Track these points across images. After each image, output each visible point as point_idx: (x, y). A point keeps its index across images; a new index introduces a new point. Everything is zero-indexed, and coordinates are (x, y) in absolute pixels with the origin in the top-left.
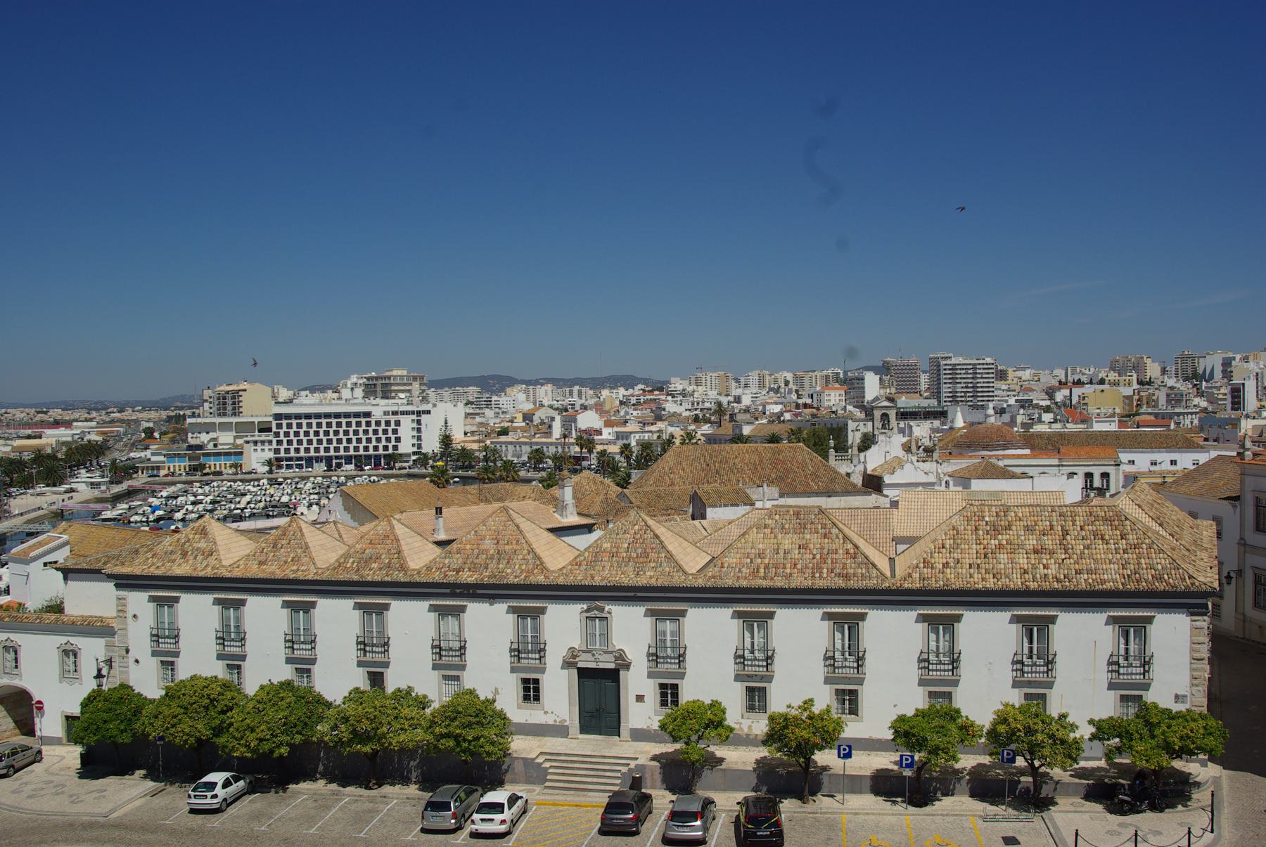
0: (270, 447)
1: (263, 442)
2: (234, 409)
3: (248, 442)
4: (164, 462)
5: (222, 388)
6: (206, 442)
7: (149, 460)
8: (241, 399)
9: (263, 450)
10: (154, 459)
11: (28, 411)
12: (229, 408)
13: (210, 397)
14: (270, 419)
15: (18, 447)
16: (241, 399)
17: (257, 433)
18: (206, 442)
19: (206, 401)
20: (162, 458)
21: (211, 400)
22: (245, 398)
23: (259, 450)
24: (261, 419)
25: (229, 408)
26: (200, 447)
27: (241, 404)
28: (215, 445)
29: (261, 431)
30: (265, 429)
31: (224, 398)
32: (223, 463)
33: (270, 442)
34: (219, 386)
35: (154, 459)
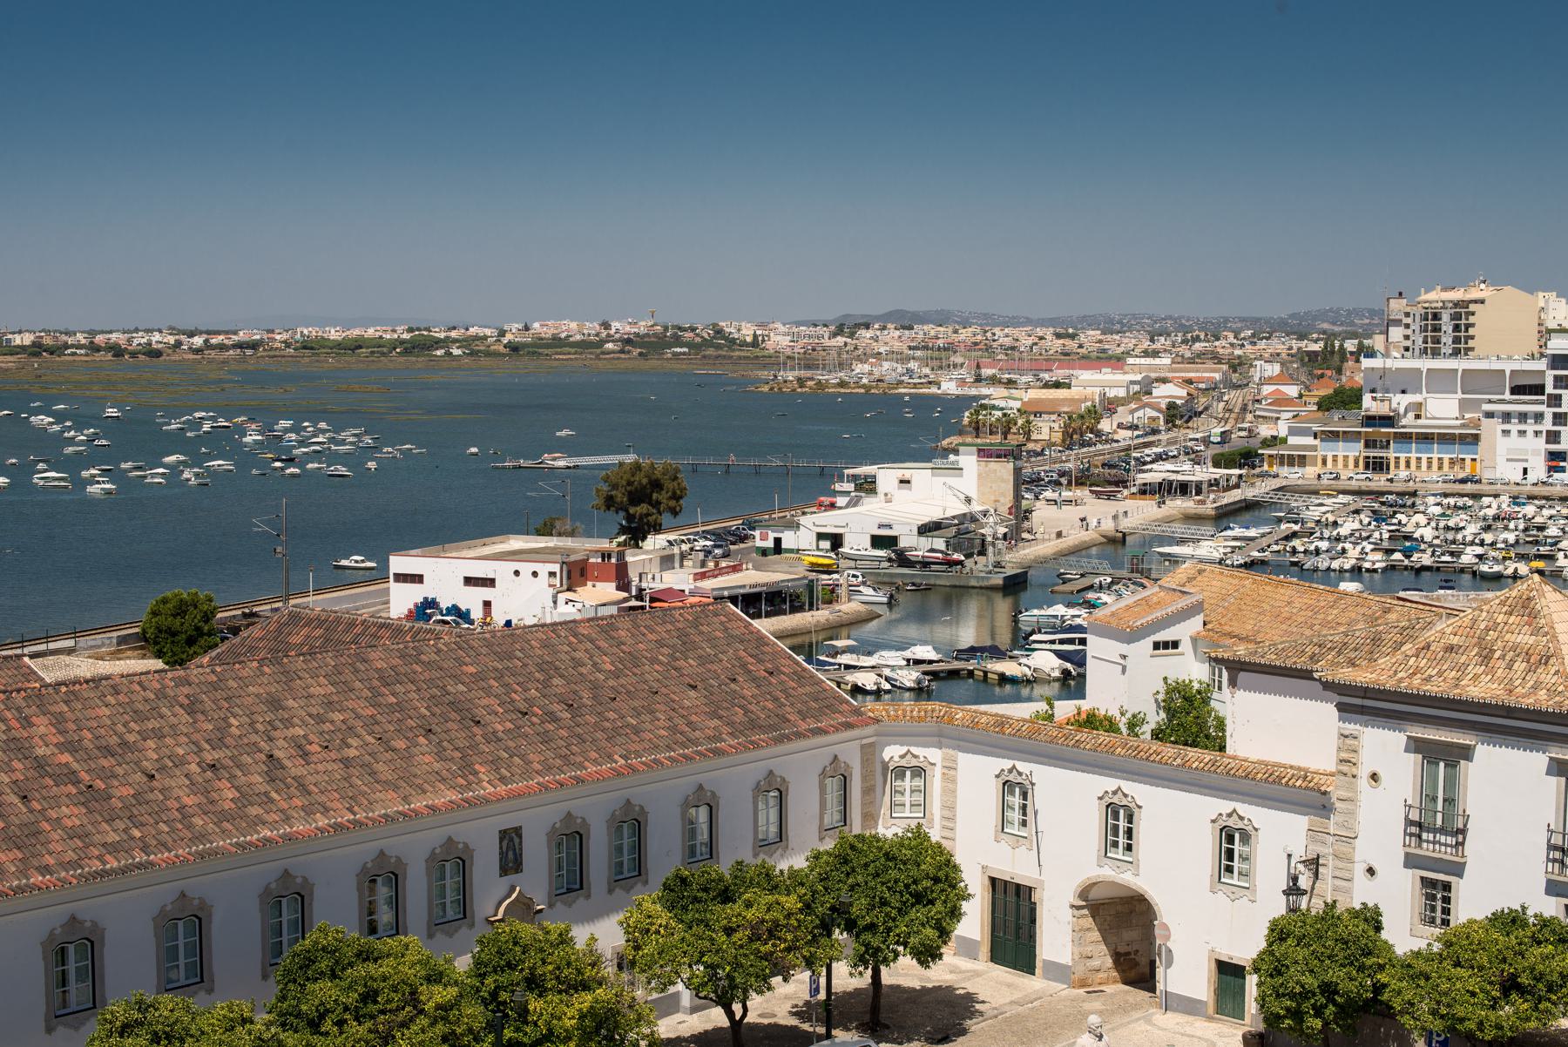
0: (1538, 428)
1: (1523, 417)
2: (1457, 340)
3: (1490, 415)
4: (1314, 448)
5: (1432, 296)
6: (1402, 411)
7: (1284, 441)
8: (1472, 319)
9: (1522, 433)
10: (1292, 440)
11: (1040, 334)
12: (1447, 339)
13: (1407, 315)
14: (1542, 365)
15: (1031, 402)
16: (1472, 319)
17: (1507, 396)
18: (1402, 411)
19: (1397, 323)
20: (1309, 441)
21: (1409, 321)
22: (1482, 320)
23: (1514, 433)
24: (1517, 366)
25: (1447, 339)
26: (1388, 421)
27: (1471, 331)
28: (1418, 417)
29: (1516, 390)
30: (1527, 388)
31: (1436, 316)
32: (1435, 456)
33: (1539, 417)
34: (1426, 293)
35: (1292, 440)
